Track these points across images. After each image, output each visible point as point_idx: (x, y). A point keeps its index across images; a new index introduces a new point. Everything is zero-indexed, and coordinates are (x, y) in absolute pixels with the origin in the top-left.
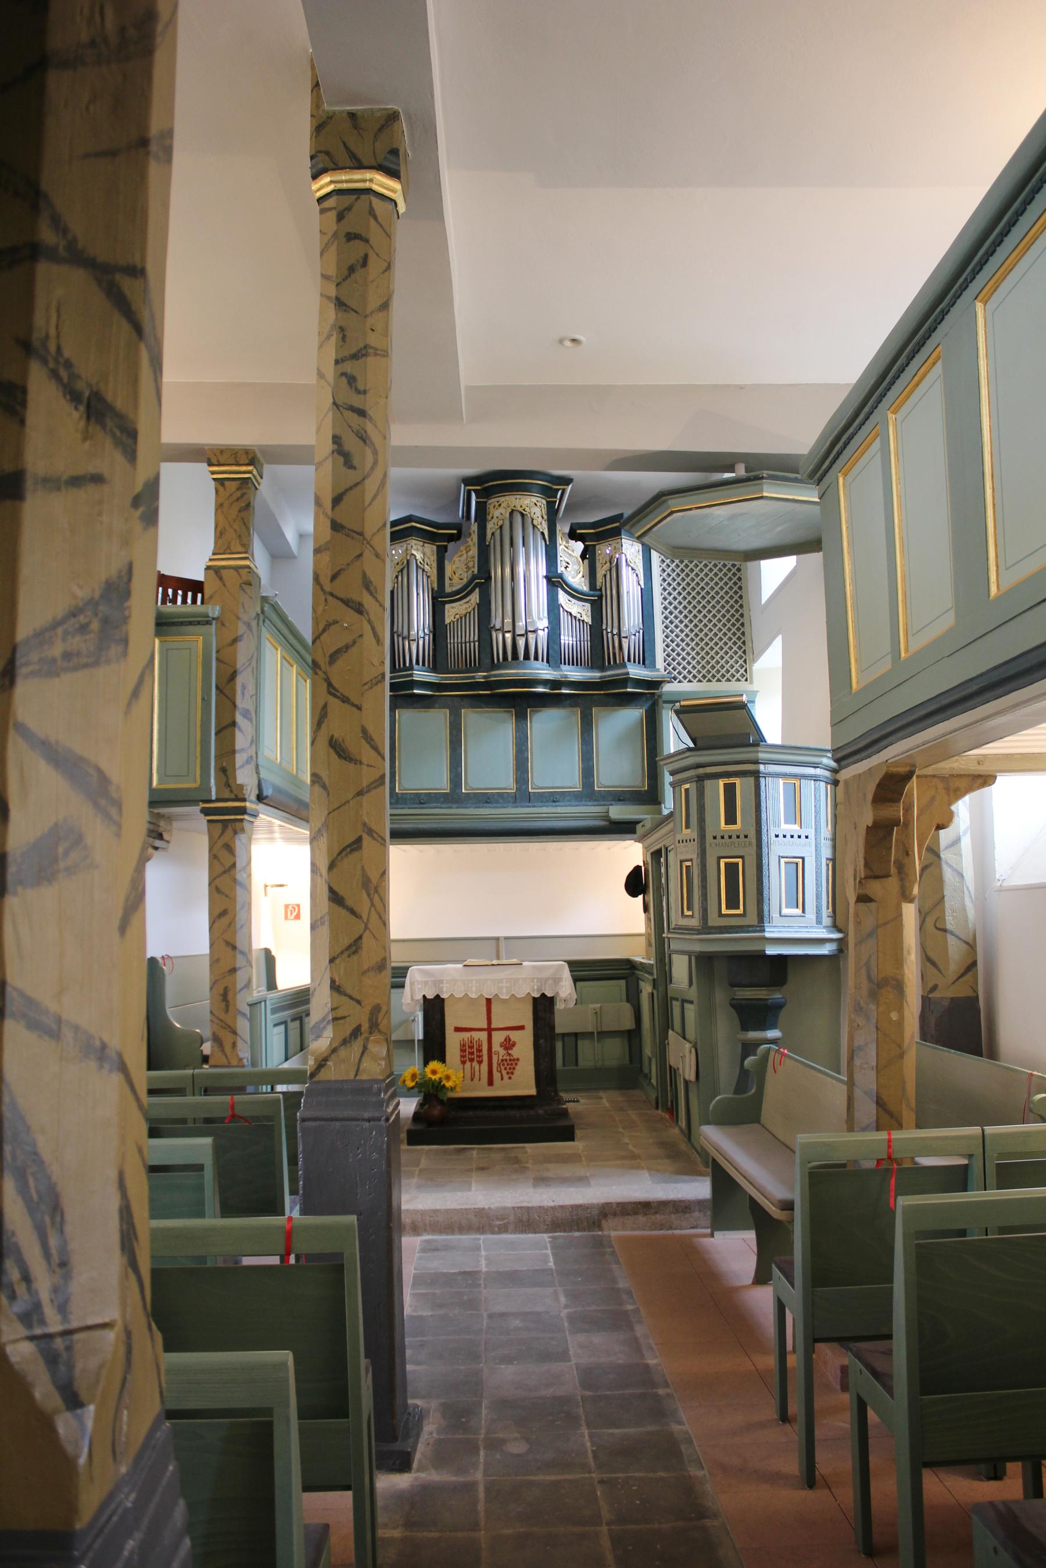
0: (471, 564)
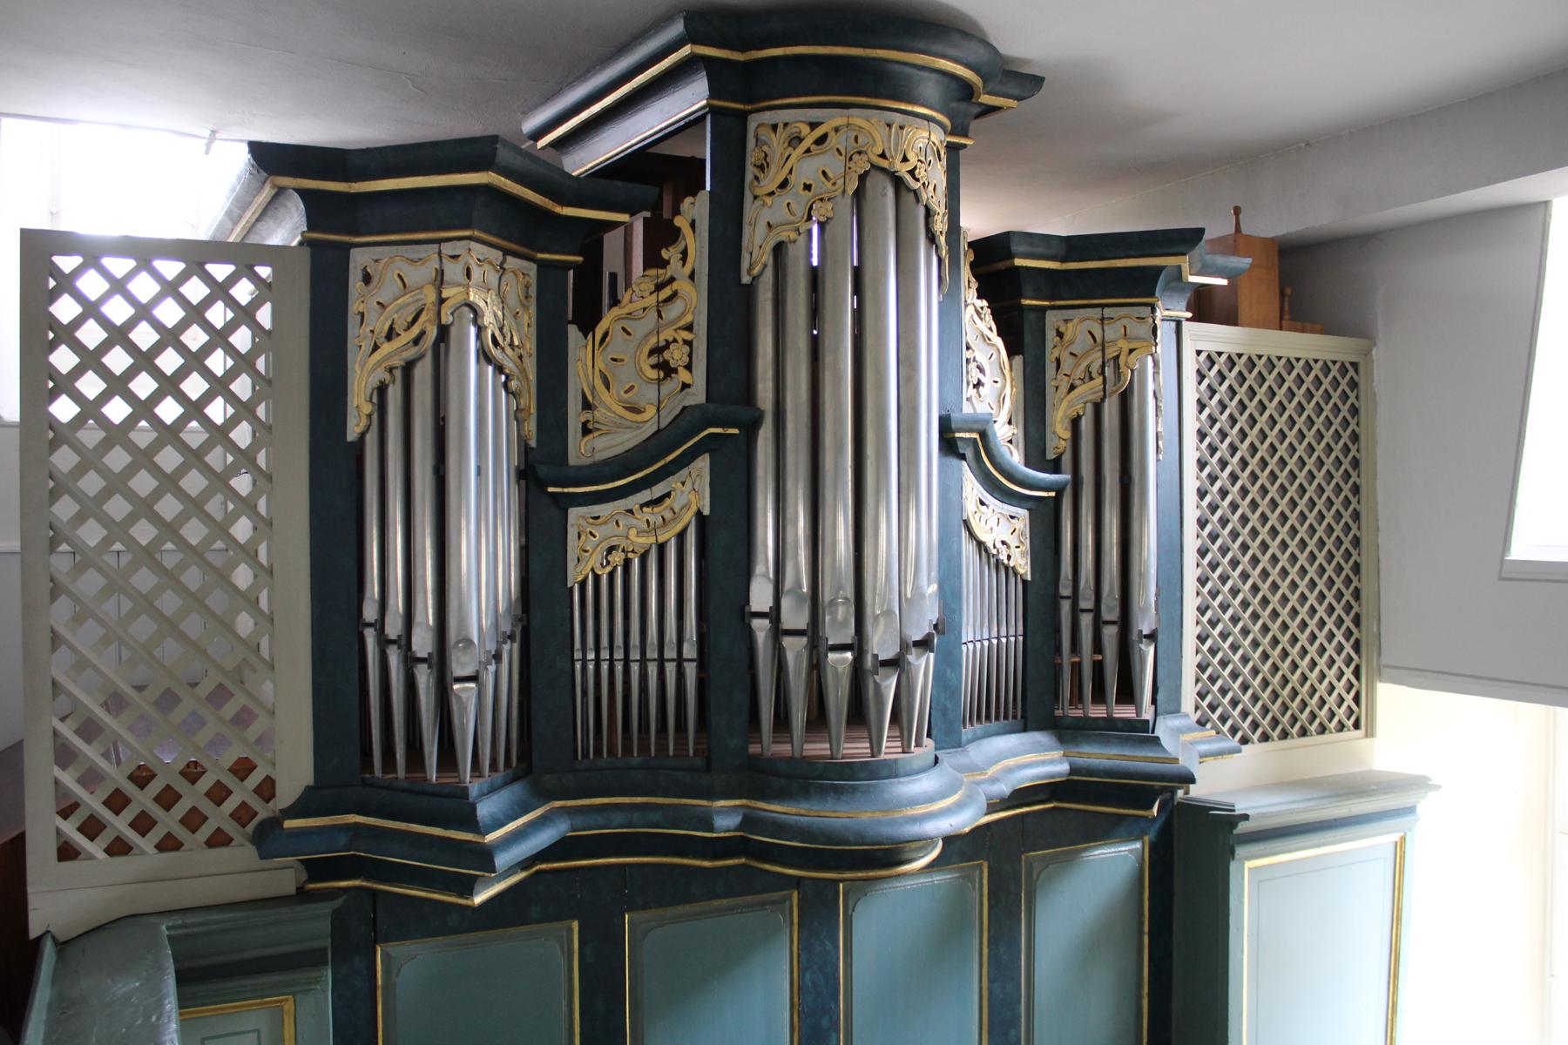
0: (676, 355)
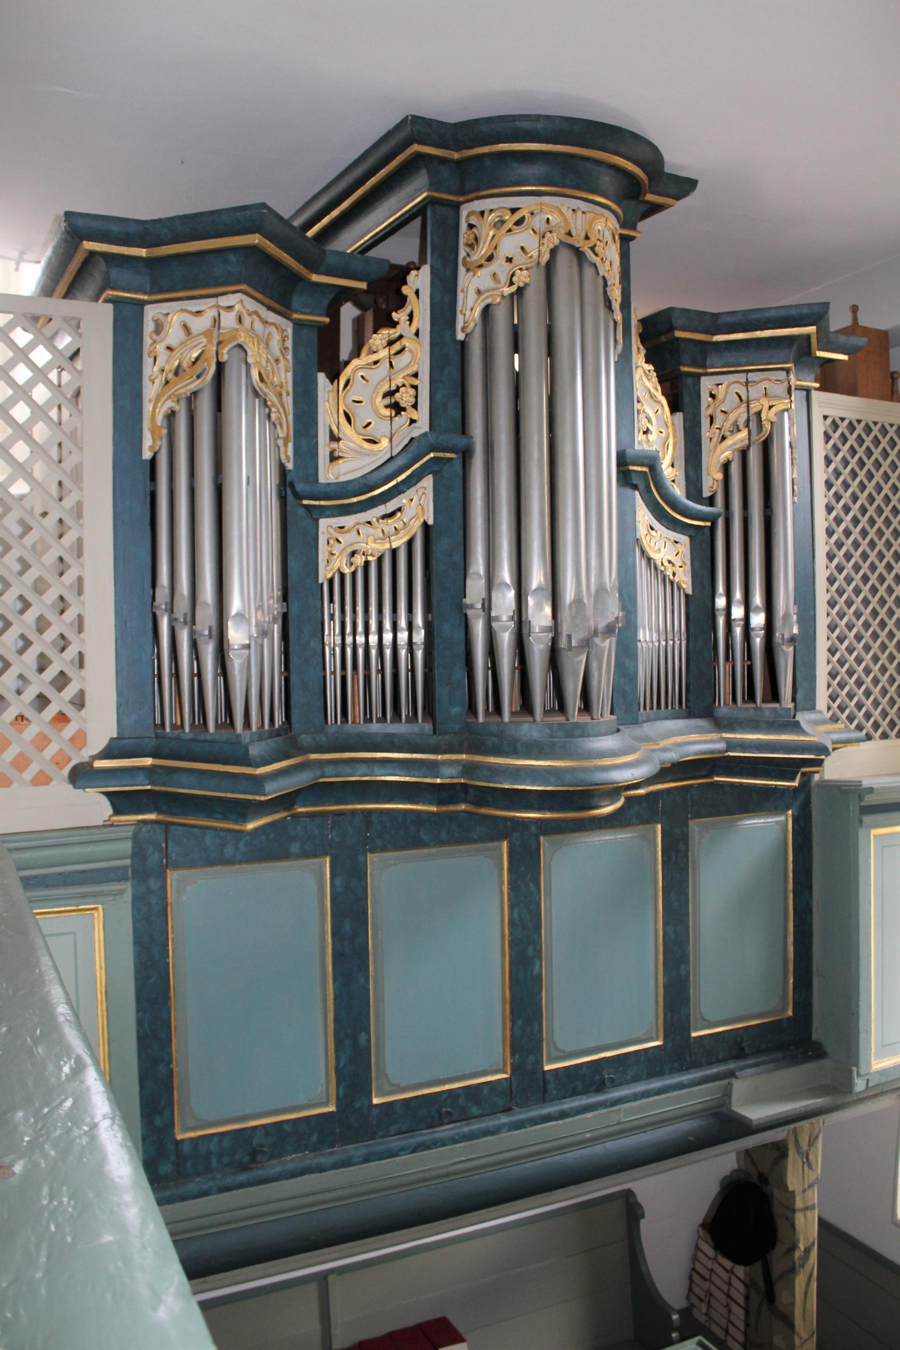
0: (405, 397)
